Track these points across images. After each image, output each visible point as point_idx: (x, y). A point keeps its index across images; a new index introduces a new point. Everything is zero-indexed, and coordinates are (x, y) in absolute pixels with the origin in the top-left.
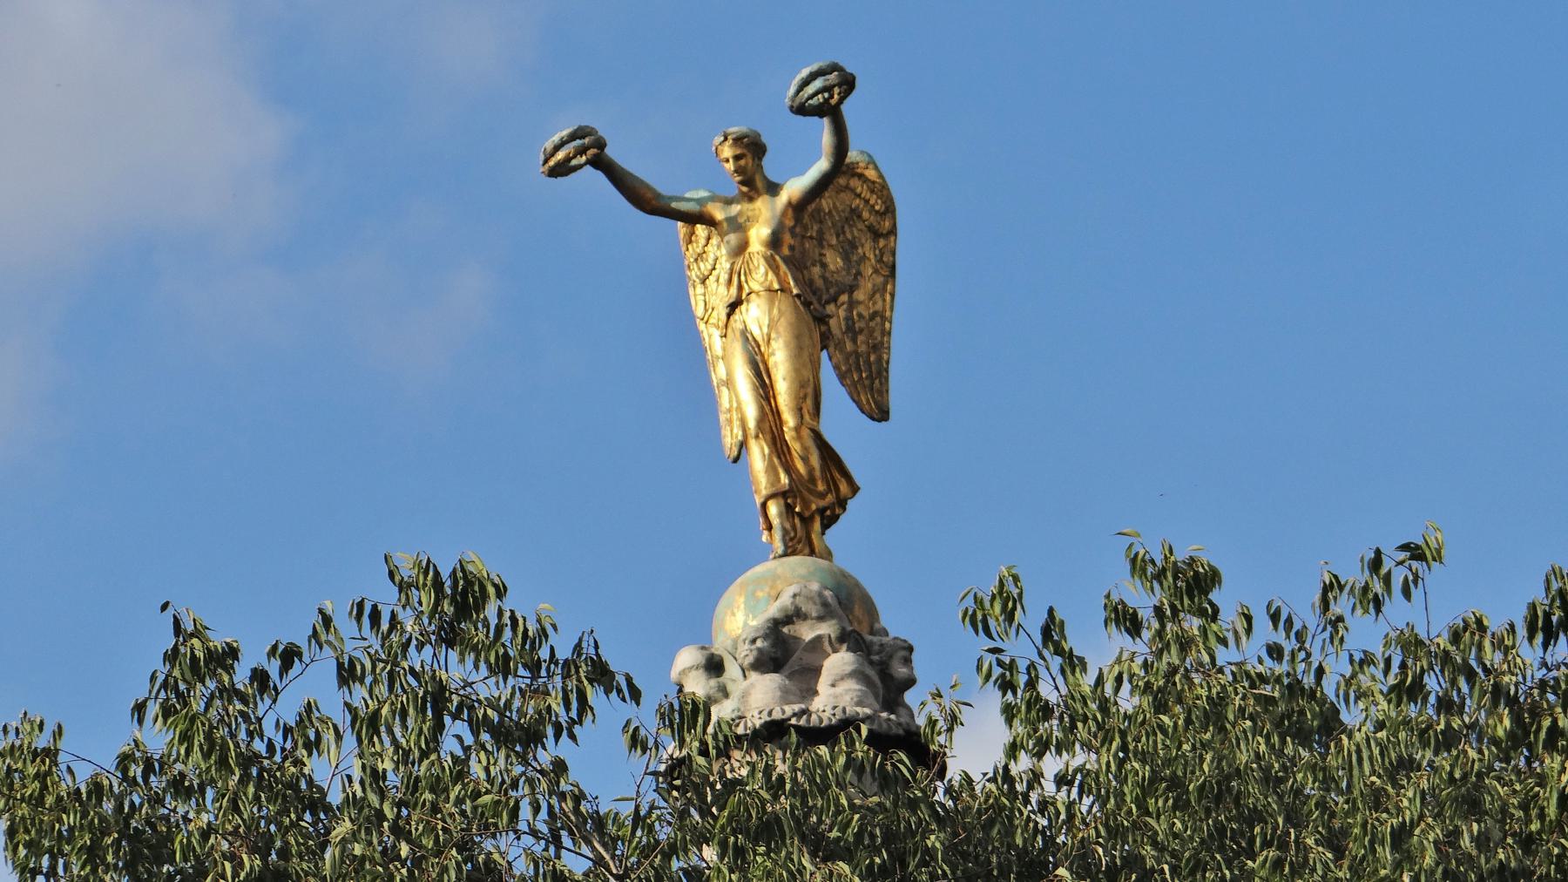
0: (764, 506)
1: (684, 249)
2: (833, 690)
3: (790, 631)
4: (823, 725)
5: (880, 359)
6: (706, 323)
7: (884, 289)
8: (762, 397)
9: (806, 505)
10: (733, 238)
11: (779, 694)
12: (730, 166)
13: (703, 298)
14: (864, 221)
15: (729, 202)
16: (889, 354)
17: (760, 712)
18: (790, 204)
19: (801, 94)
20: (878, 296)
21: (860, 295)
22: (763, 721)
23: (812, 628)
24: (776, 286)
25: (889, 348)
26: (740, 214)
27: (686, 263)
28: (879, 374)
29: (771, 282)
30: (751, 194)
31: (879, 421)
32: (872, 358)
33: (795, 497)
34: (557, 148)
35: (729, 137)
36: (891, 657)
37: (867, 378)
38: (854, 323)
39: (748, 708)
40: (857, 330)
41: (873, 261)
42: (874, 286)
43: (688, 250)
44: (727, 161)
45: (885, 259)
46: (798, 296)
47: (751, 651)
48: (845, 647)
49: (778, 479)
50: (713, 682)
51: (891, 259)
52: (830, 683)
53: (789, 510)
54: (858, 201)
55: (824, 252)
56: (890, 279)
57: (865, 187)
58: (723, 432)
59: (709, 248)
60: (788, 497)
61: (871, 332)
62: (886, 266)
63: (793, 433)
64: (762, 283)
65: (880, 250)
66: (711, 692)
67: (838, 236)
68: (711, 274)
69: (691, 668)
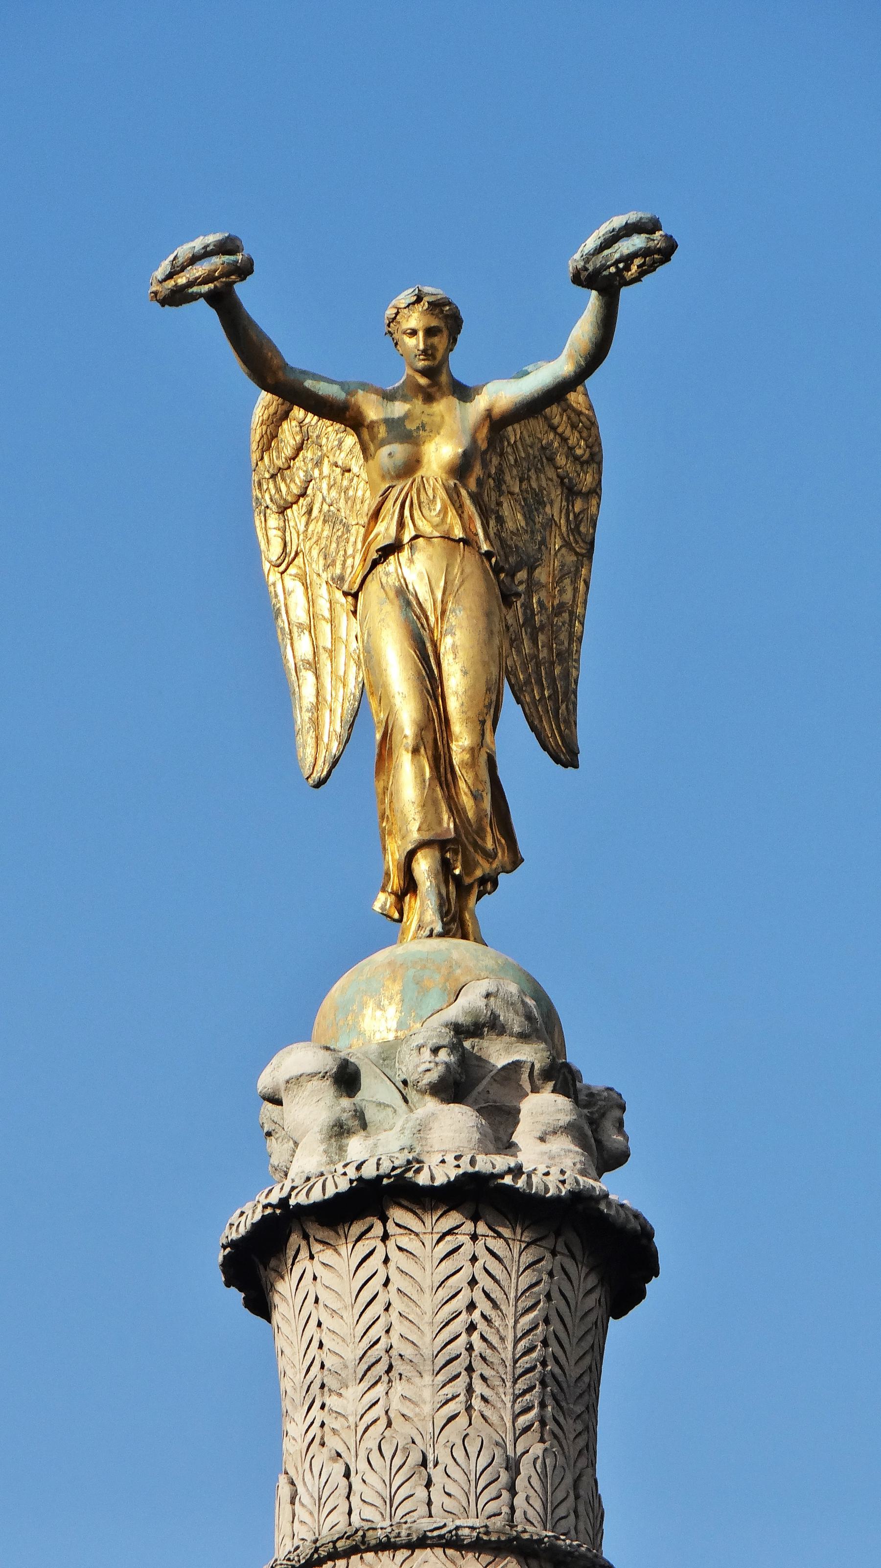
0: (411, 856)
1: (255, 456)
2: (544, 1147)
3: (473, 1047)
4: (548, 1195)
5: (566, 675)
6: (282, 573)
7: (577, 572)
8: (428, 691)
9: (468, 867)
10: (399, 451)
11: (477, 1136)
12: (415, 343)
13: (280, 533)
14: (557, 468)
15: (389, 397)
16: (578, 669)
17: (458, 1158)
18: (489, 414)
19: (606, 252)
20: (567, 581)
21: (542, 575)
22: (461, 1171)
23: (507, 1050)
24: (458, 533)
25: (577, 661)
26: (407, 416)
27: (255, 478)
28: (566, 694)
29: (451, 527)
30: (432, 390)
31: (565, 766)
32: (557, 671)
33: (456, 852)
34: (194, 259)
35: (426, 299)
36: (603, 1115)
37: (550, 697)
38: (533, 615)
39: (426, 1149)
40: (538, 624)
41: (564, 529)
42: (563, 565)
43: (262, 459)
44: (414, 333)
45: (583, 529)
46: (488, 555)
47: (437, 1064)
48: (551, 1085)
49: (440, 822)
50: (346, 1102)
51: (591, 531)
52: (539, 1134)
53: (445, 867)
54: (552, 436)
55: (502, 499)
56: (586, 562)
57: (565, 418)
58: (299, 740)
59: (298, 462)
60: (448, 850)
61: (554, 636)
62: (584, 541)
63: (466, 756)
64: (437, 525)
65: (576, 516)
66: (345, 1116)
67: (521, 481)
68: (296, 502)
69: (313, 1075)
